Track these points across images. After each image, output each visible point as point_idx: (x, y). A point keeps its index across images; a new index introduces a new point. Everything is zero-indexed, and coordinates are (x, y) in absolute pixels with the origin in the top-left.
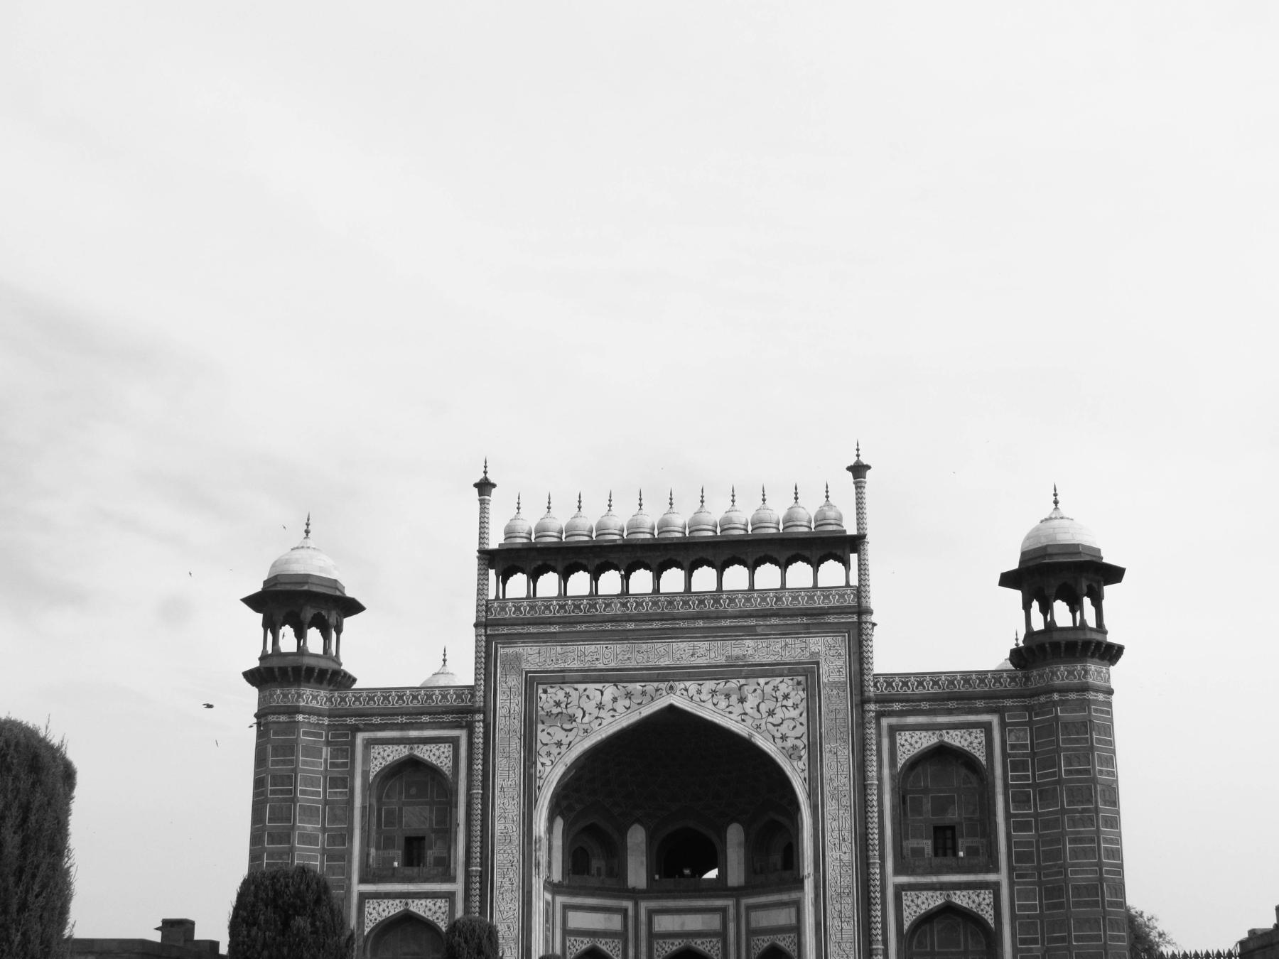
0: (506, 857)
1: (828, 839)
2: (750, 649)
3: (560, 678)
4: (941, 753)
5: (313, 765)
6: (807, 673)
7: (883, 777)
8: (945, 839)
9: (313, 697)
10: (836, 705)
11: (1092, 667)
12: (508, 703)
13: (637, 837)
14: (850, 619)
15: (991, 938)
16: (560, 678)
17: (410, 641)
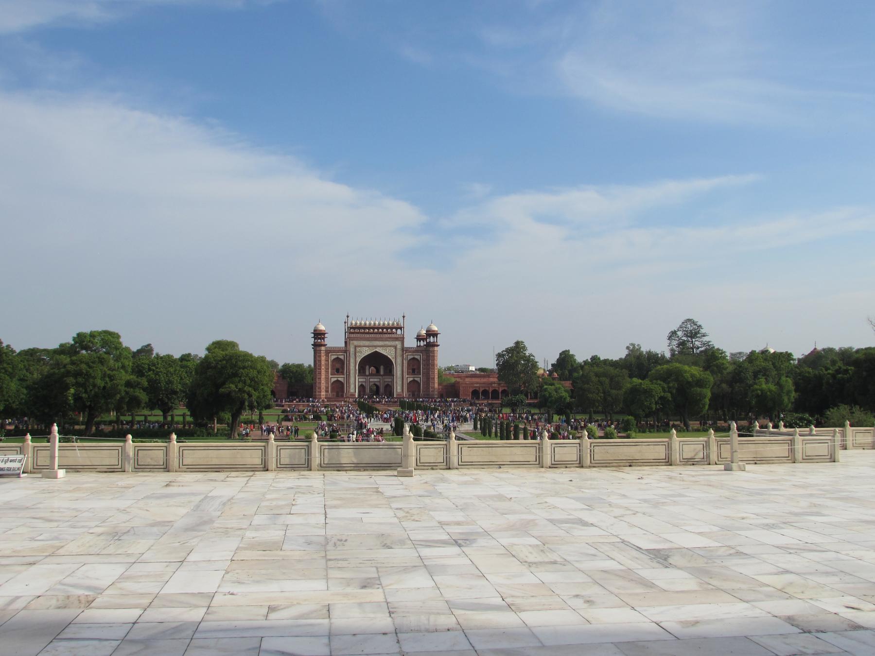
0: (352, 372)
1: (398, 370)
2: (387, 343)
3: (360, 346)
4: (414, 358)
5: (323, 358)
6: (395, 347)
7: (405, 362)
8: (414, 370)
9: (323, 348)
10: (399, 352)
11: (436, 348)
12: (352, 350)
13: (367, 367)
14: (402, 339)
15: (419, 384)
16: (360, 346)
17: (335, 340)
